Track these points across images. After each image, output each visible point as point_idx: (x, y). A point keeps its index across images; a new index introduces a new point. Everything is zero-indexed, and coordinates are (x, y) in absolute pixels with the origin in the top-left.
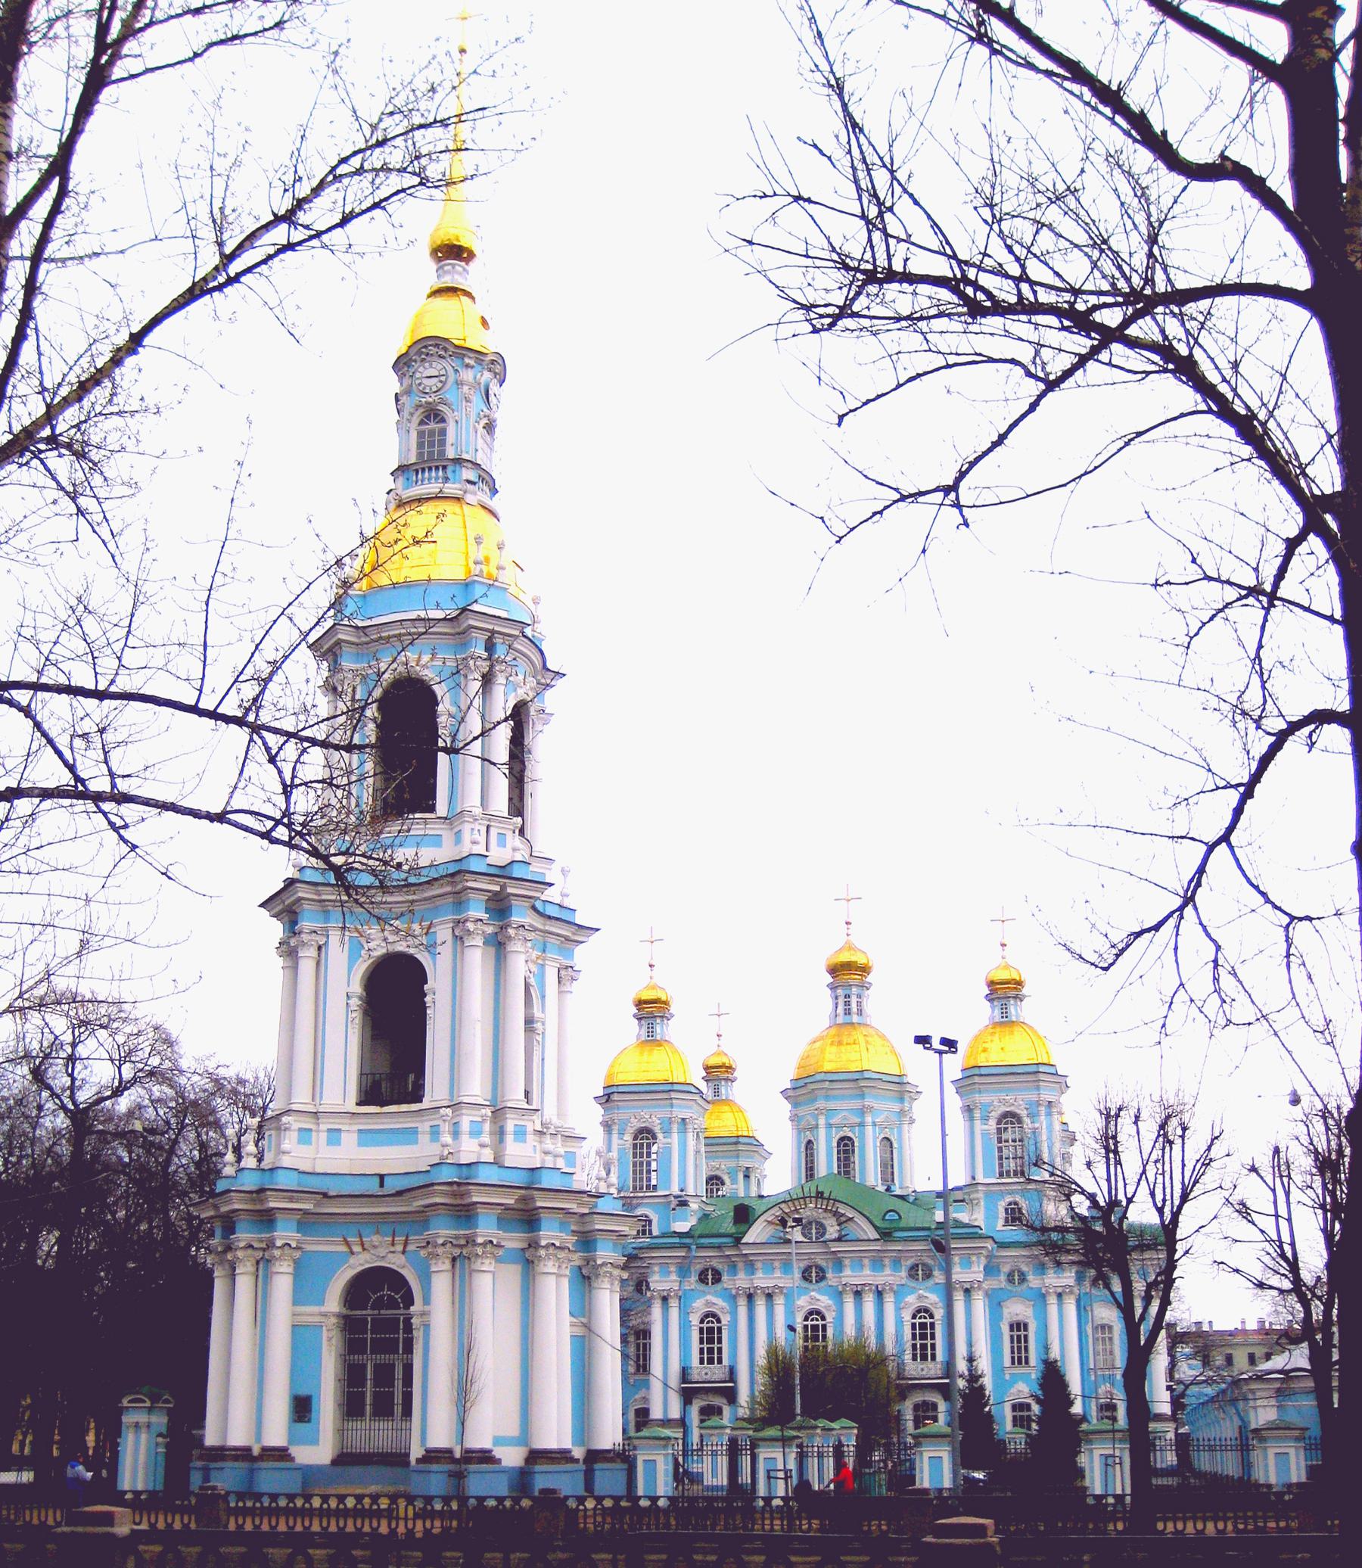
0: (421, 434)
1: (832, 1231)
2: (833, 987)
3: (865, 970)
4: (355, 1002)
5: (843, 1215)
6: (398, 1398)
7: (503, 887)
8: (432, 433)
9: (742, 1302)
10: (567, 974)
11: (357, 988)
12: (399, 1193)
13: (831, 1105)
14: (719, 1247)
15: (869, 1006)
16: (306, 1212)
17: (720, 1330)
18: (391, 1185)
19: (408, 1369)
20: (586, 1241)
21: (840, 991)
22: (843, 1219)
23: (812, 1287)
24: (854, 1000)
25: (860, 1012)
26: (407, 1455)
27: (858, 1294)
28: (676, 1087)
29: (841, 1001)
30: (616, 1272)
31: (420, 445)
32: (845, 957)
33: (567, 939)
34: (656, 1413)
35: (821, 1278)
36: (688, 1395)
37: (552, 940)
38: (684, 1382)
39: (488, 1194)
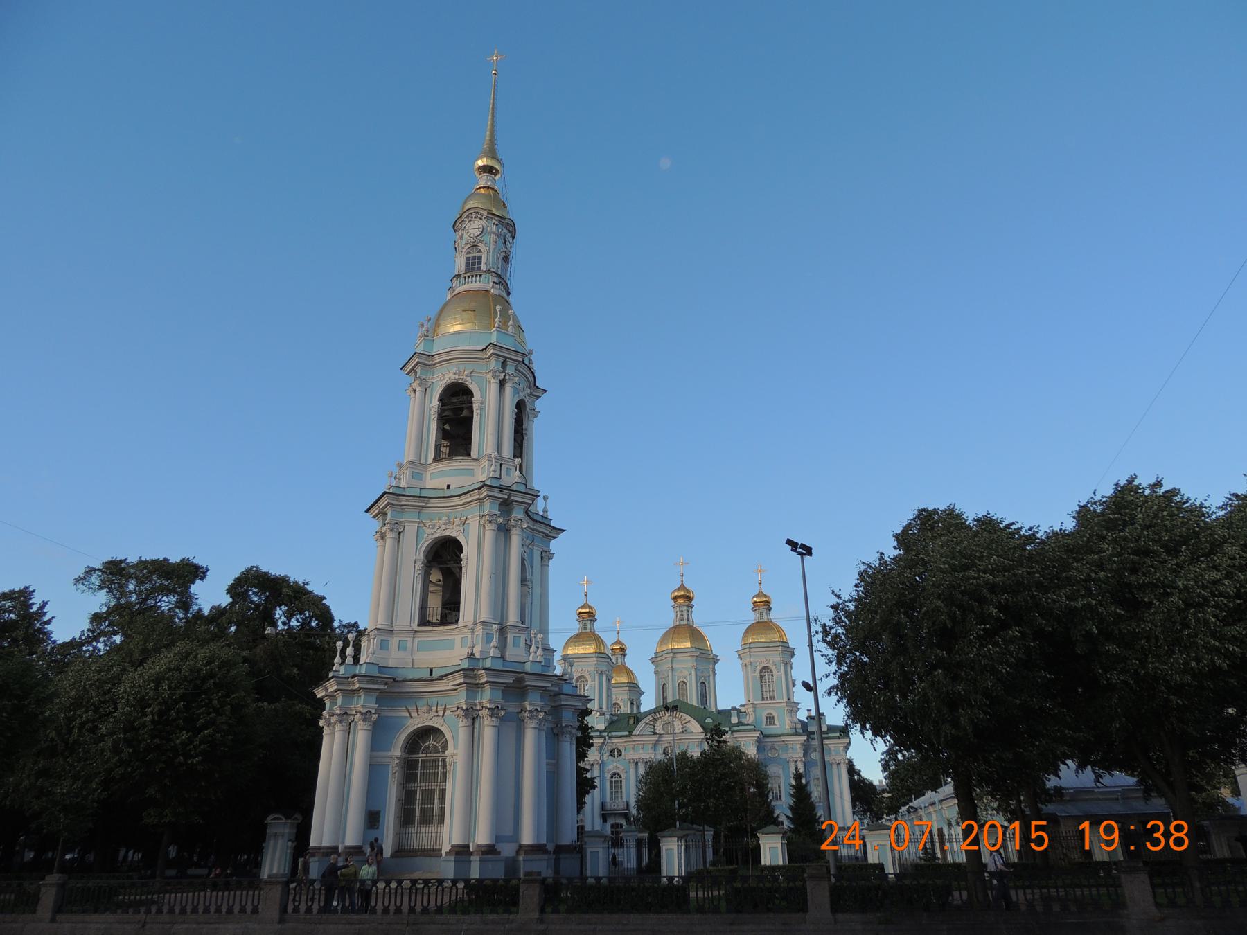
0: (468, 259)
1: (678, 729)
4: (419, 565)
6: (436, 812)
7: (509, 496)
8: (474, 258)
9: (632, 766)
10: (546, 556)
11: (421, 557)
12: (442, 677)
16: (382, 691)
18: (436, 673)
19: (443, 792)
20: (556, 710)
26: (440, 850)
30: (574, 731)
31: (467, 265)
33: (547, 535)
34: (588, 828)
36: (604, 818)
37: (538, 535)
39: (497, 676)
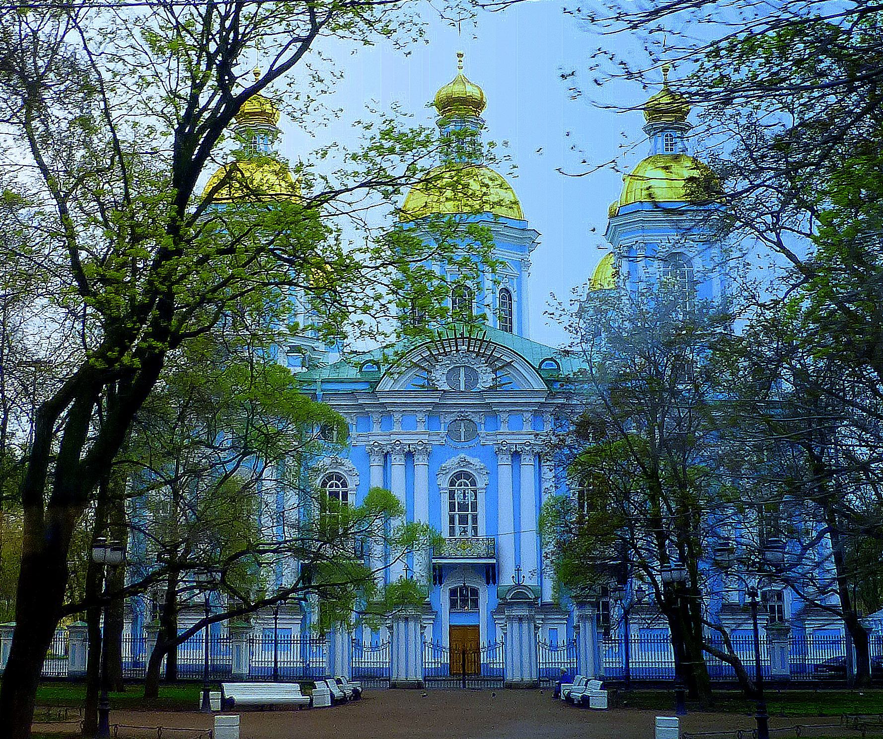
3: (479, 105)
9: (376, 461)
14: (352, 394)
17: (345, 495)
27: (516, 455)
32: (458, 90)
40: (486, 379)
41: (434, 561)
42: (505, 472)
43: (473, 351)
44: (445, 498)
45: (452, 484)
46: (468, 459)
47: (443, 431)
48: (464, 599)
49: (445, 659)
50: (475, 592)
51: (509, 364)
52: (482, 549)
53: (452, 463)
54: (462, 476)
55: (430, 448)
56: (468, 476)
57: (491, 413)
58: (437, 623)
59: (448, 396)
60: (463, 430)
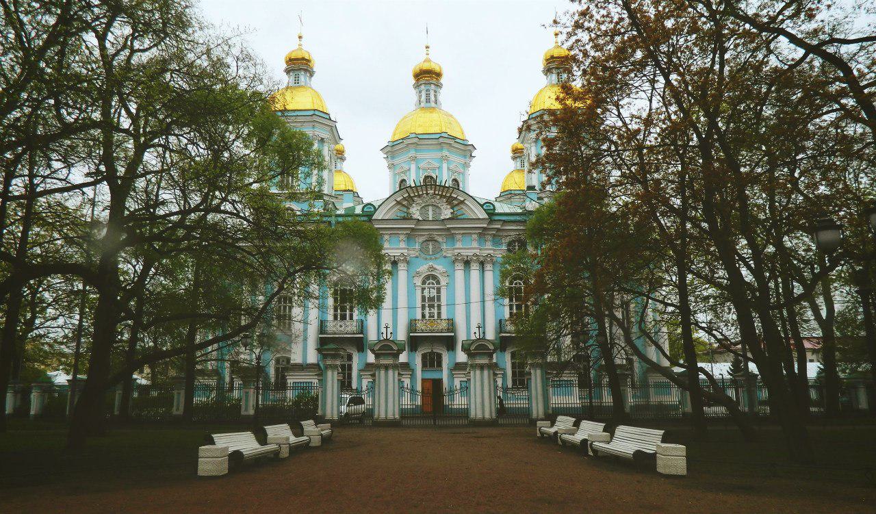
2: (417, 86)
3: (439, 75)
5: (456, 199)
13: (419, 155)
15: (441, 98)
21: (423, 87)
22: (455, 202)
23: (428, 257)
24: (432, 93)
25: (436, 102)
27: (467, 263)
28: (317, 113)
29: (424, 94)
32: (426, 66)
35: (438, 250)
38: (321, 333)
40: (447, 213)
41: (411, 334)
42: (459, 274)
43: (438, 195)
44: (419, 293)
45: (424, 283)
46: (435, 266)
47: (417, 246)
48: (432, 361)
49: (419, 402)
50: (439, 356)
51: (462, 202)
52: (444, 325)
53: (423, 268)
54: (431, 278)
55: (408, 258)
56: (434, 277)
57: (450, 234)
58: (413, 377)
59: (421, 223)
60: (431, 247)
